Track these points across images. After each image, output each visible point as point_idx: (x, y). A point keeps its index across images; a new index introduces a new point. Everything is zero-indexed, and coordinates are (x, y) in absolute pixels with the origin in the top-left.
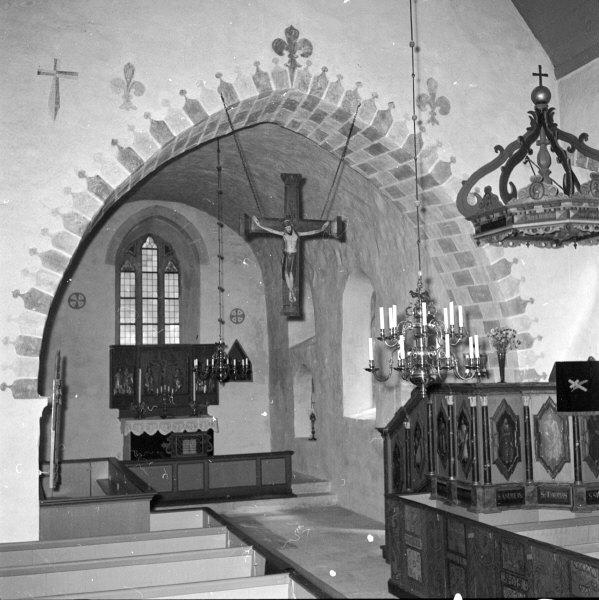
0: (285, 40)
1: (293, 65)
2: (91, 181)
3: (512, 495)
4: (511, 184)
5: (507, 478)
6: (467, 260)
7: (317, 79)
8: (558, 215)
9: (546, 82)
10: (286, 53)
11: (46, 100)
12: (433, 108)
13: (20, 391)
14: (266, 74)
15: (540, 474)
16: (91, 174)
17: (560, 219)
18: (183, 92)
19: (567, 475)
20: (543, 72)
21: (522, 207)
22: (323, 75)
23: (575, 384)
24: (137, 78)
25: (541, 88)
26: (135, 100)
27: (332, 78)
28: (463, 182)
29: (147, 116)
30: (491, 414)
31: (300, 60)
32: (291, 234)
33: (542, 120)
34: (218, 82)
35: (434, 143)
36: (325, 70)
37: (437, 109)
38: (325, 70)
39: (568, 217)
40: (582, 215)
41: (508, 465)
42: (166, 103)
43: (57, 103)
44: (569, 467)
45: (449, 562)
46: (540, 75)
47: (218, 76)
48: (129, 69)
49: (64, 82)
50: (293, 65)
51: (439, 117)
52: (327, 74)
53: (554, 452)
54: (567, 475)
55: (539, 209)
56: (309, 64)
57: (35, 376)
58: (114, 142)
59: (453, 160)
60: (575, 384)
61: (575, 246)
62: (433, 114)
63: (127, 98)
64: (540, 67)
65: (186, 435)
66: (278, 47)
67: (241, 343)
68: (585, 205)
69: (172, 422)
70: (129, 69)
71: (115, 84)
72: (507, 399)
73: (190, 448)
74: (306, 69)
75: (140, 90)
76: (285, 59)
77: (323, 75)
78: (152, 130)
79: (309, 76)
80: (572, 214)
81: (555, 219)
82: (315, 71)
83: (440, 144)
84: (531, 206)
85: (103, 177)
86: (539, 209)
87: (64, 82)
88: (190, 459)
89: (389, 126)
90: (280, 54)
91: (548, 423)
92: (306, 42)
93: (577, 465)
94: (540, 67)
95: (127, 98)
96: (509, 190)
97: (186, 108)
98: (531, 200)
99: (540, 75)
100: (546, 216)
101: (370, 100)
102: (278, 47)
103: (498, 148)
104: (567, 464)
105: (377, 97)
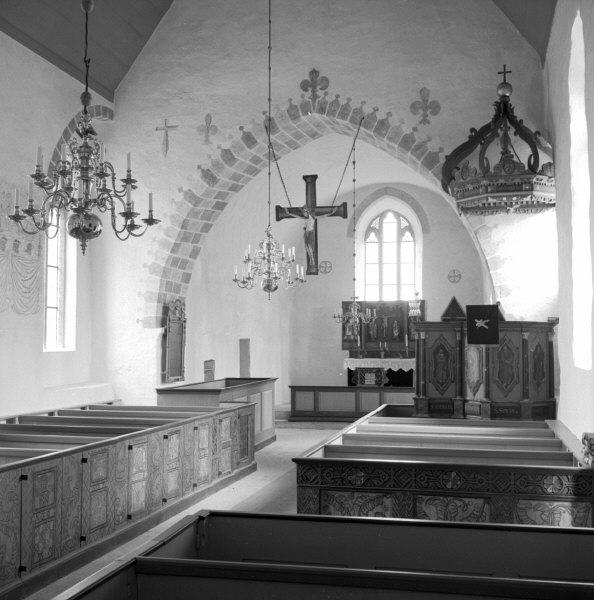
0: (309, 79)
1: (315, 97)
2: (186, 193)
11: (159, 146)
13: (146, 324)
14: (296, 107)
15: (469, 396)
16: (185, 189)
17: (483, 193)
18: (241, 128)
19: (481, 395)
22: (336, 100)
23: (480, 323)
24: (213, 123)
25: (505, 84)
26: (211, 138)
27: (343, 101)
29: (219, 147)
31: (320, 93)
32: (307, 218)
33: (504, 110)
35: (424, 138)
36: (338, 96)
38: (338, 96)
39: (487, 192)
41: (442, 384)
42: (231, 137)
43: (167, 146)
48: (208, 118)
49: (171, 133)
50: (315, 97)
51: (431, 118)
56: (326, 94)
58: (199, 167)
60: (480, 323)
63: (207, 137)
65: (369, 370)
68: (501, 181)
70: (208, 118)
71: (200, 129)
73: (370, 379)
75: (215, 129)
76: (309, 94)
77: (336, 100)
78: (223, 156)
79: (326, 103)
80: (489, 190)
82: (330, 99)
83: (429, 139)
85: (194, 191)
87: (171, 133)
88: (370, 389)
90: (306, 90)
92: (325, 80)
95: (207, 137)
101: (372, 114)
102: (304, 86)
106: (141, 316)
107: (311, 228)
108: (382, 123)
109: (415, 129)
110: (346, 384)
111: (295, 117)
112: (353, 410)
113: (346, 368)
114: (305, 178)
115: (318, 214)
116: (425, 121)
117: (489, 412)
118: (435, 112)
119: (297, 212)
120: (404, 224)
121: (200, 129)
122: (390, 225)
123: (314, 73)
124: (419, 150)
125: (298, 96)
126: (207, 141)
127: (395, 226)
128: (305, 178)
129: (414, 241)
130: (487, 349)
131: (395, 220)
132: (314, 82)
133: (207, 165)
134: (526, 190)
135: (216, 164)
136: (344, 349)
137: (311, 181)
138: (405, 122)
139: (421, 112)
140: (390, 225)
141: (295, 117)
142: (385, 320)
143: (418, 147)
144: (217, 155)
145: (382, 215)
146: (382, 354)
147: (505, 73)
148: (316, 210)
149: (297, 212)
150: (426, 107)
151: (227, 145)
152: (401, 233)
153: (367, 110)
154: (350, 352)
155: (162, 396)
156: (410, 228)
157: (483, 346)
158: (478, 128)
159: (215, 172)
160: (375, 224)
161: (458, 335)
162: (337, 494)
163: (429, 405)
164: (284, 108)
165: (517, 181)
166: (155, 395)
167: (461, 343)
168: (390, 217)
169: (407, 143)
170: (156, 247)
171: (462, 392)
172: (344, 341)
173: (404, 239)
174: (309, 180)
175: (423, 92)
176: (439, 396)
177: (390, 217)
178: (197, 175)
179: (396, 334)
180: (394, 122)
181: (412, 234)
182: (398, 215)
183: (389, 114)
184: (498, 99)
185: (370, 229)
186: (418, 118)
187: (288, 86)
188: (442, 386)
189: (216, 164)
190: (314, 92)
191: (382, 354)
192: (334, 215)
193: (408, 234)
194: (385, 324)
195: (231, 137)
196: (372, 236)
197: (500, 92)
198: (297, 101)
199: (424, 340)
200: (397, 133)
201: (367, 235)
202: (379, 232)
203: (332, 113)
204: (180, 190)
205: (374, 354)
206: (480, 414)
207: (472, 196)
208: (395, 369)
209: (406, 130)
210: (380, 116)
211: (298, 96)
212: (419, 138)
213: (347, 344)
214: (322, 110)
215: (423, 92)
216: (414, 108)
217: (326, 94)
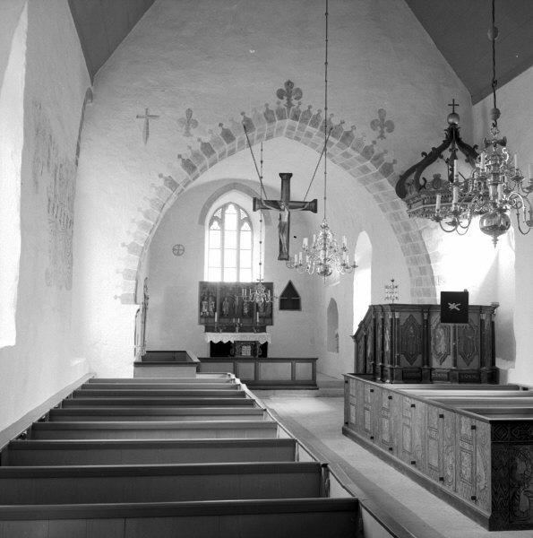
1: (289, 105)
2: (166, 180)
4: (424, 179)
5: (411, 364)
6: (407, 228)
7: (304, 113)
10: (285, 98)
11: (141, 134)
13: (124, 300)
14: (272, 111)
15: (435, 364)
18: (221, 125)
22: (309, 111)
23: (452, 306)
24: (193, 117)
25: (454, 114)
26: (192, 131)
27: (314, 112)
28: (400, 176)
29: (199, 140)
30: (402, 323)
31: (295, 102)
33: (453, 135)
34: (242, 118)
36: (310, 107)
37: (386, 128)
38: (310, 107)
42: (211, 132)
43: (148, 134)
44: (450, 358)
45: (366, 409)
47: (243, 114)
49: (151, 122)
50: (289, 105)
51: (386, 134)
52: (311, 110)
53: (442, 348)
54: (448, 364)
56: (300, 104)
57: (132, 292)
58: (180, 156)
59: (395, 162)
60: (452, 306)
62: (382, 132)
63: (188, 129)
65: (246, 343)
66: (280, 94)
67: (297, 286)
69: (229, 334)
70: (189, 112)
71: (181, 121)
73: (246, 351)
74: (297, 108)
75: (196, 124)
76: (284, 101)
77: (309, 111)
78: (202, 149)
82: (303, 108)
83: (386, 152)
85: (174, 179)
87: (151, 122)
88: (246, 360)
90: (282, 98)
92: (298, 90)
93: (455, 356)
95: (188, 129)
96: (422, 182)
97: (222, 134)
99: (454, 105)
102: (280, 94)
103: (424, 154)
106: (120, 292)
107: (285, 220)
108: (347, 134)
109: (374, 142)
110: (209, 356)
111: (271, 121)
112: (309, 377)
113: (209, 341)
114: (281, 175)
115: (291, 208)
116: (382, 136)
118: (390, 130)
119: (275, 204)
120: (244, 215)
121: (181, 121)
122: (231, 216)
123: (289, 84)
124: (377, 160)
125: (274, 103)
126: (188, 134)
127: (235, 216)
128: (281, 175)
129: (252, 230)
130: (454, 327)
131: (235, 211)
132: (288, 91)
133: (187, 155)
135: (196, 155)
136: (201, 324)
137: (286, 178)
138: (367, 136)
140: (231, 216)
141: (271, 121)
142: (237, 299)
143: (376, 158)
144: (197, 147)
145: (225, 207)
146: (237, 329)
147: (454, 105)
148: (290, 204)
149: (275, 204)
150: (383, 125)
151: (207, 139)
152: (240, 223)
153: (335, 122)
154: (206, 327)
155: (139, 369)
156: (248, 219)
157: (451, 325)
159: (194, 162)
160: (218, 214)
161: (425, 315)
162: (521, 448)
164: (261, 112)
166: (132, 367)
167: (427, 323)
168: (231, 209)
169: (367, 153)
170: (135, 228)
171: (427, 361)
172: (201, 317)
173: (242, 229)
174: (285, 177)
177: (231, 209)
178: (178, 164)
179: (246, 311)
180: (357, 134)
181: (251, 225)
182: (238, 207)
183: (353, 127)
184: (447, 126)
185: (214, 218)
186: (377, 133)
187: (264, 91)
188: (411, 359)
189: (196, 155)
190: (289, 100)
191: (237, 329)
192: (306, 209)
193: (246, 225)
194: (237, 303)
195: (211, 132)
196: (215, 224)
197: (451, 120)
198: (273, 107)
200: (359, 144)
201: (211, 224)
202: (221, 221)
203: (305, 121)
204: (161, 176)
205: (231, 329)
206: (448, 380)
208: (225, 342)
209: (368, 143)
210: (346, 128)
211: (274, 103)
212: (377, 150)
213: (203, 320)
214: (296, 118)
217: (300, 104)
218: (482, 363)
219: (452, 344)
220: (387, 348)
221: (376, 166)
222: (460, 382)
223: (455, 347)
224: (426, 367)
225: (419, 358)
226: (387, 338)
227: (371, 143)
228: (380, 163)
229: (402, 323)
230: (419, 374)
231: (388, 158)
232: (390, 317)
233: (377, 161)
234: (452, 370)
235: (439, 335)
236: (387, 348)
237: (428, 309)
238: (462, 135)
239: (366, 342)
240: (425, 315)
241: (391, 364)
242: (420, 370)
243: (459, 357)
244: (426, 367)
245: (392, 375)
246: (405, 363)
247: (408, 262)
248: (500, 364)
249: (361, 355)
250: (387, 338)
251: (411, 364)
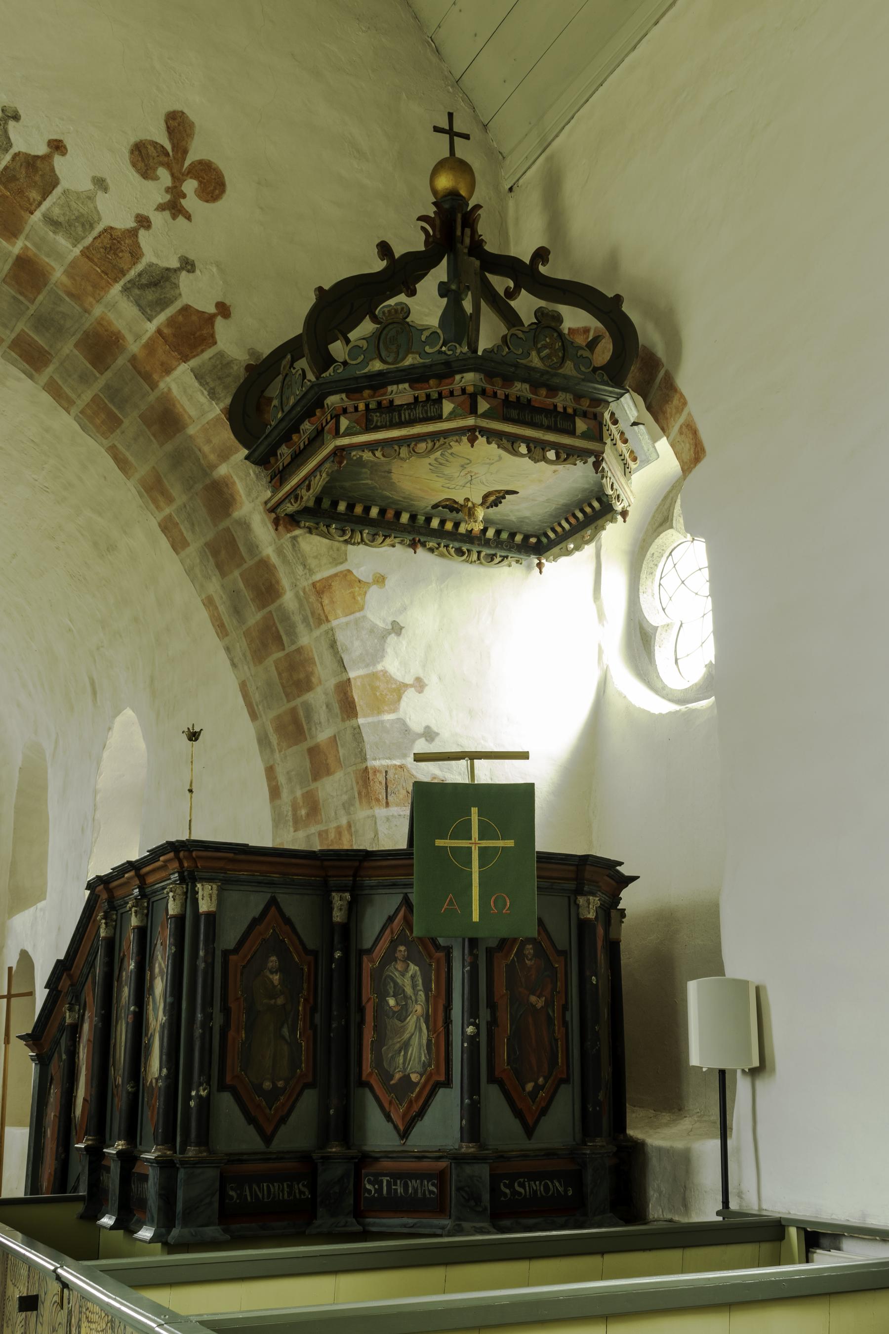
3: (275, 1188)
5: (268, 1139)
6: (265, 588)
8: (448, 407)
9: (463, 150)
12: (178, 179)
17: (452, 416)
19: (441, 1126)
20: (456, 129)
21: (353, 387)
33: (453, 226)
39: (473, 411)
40: (514, 413)
46: (451, 133)
51: (191, 202)
55: (401, 394)
59: (224, 310)
61: (540, 565)
64: (450, 115)
68: (521, 389)
72: (280, 898)
80: (483, 406)
81: (439, 418)
83: (188, 265)
84: (378, 381)
86: (401, 394)
89: (45, 195)
91: (395, 971)
94: (450, 115)
98: (377, 366)
99: (451, 133)
100: (419, 412)
104: (442, 1092)
105: (16, 117)
109: (144, 222)
116: (174, 207)
117: (486, 1197)
134: (585, 436)
139: (164, 176)
158: (399, 251)
161: (339, 902)
163: (224, 1180)
165: (562, 400)
171: (342, 1125)
175: (178, 125)
176: (258, 1144)
199: (210, 916)
206: (439, 1207)
207: (411, 423)
209: (115, 213)
215: (178, 125)
216: (144, 157)
218: (587, 1125)
219: (461, 1029)
220: (155, 1066)
221: (148, 310)
222: (504, 1213)
223: (473, 1040)
224: (334, 1149)
225: (309, 1101)
226: (157, 1017)
227: (131, 224)
228: (162, 304)
229: (229, 937)
230: (301, 1189)
231: (197, 293)
232: (173, 908)
233: (150, 295)
234: (458, 1159)
235: (399, 992)
236: (155, 1066)
237: (347, 871)
238: (484, 229)
239: (73, 1054)
240: (339, 902)
241: (168, 1139)
242: (308, 1165)
243: (492, 1096)
244: (334, 1149)
245: (168, 1195)
246: (234, 1132)
247: (263, 741)
248: (658, 1136)
249: (52, 1114)
250: (157, 1017)
251: (268, 1139)
